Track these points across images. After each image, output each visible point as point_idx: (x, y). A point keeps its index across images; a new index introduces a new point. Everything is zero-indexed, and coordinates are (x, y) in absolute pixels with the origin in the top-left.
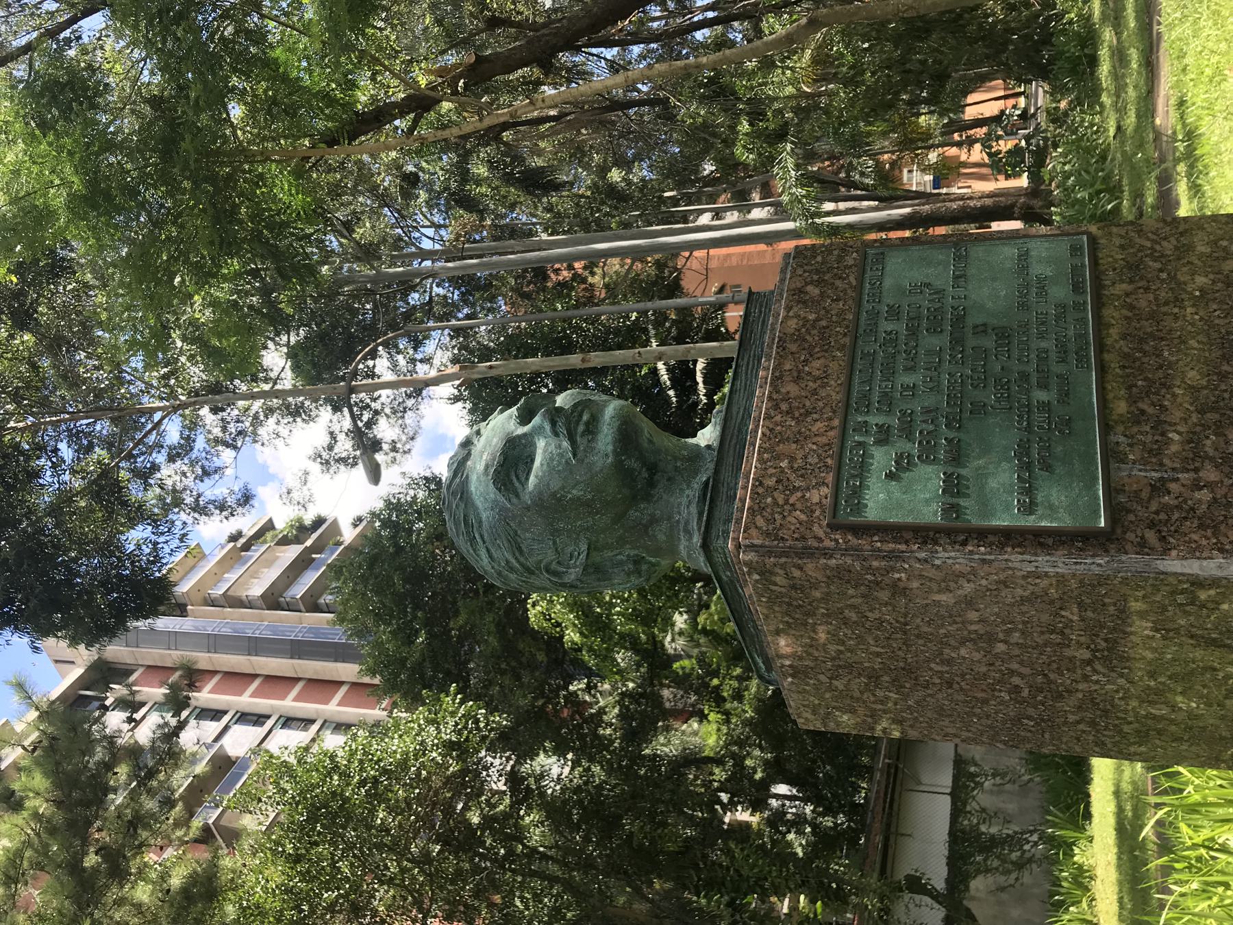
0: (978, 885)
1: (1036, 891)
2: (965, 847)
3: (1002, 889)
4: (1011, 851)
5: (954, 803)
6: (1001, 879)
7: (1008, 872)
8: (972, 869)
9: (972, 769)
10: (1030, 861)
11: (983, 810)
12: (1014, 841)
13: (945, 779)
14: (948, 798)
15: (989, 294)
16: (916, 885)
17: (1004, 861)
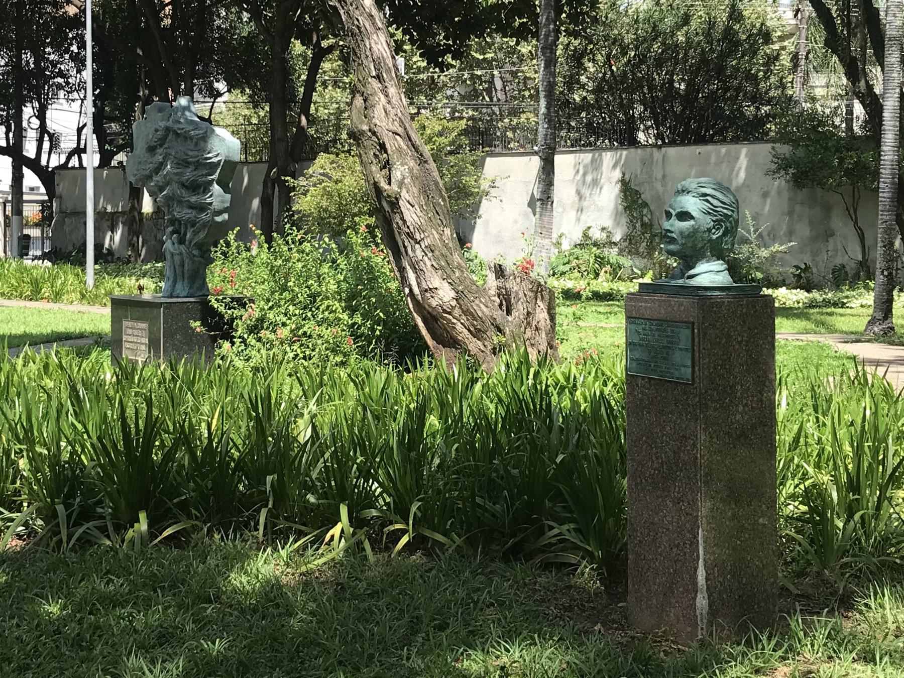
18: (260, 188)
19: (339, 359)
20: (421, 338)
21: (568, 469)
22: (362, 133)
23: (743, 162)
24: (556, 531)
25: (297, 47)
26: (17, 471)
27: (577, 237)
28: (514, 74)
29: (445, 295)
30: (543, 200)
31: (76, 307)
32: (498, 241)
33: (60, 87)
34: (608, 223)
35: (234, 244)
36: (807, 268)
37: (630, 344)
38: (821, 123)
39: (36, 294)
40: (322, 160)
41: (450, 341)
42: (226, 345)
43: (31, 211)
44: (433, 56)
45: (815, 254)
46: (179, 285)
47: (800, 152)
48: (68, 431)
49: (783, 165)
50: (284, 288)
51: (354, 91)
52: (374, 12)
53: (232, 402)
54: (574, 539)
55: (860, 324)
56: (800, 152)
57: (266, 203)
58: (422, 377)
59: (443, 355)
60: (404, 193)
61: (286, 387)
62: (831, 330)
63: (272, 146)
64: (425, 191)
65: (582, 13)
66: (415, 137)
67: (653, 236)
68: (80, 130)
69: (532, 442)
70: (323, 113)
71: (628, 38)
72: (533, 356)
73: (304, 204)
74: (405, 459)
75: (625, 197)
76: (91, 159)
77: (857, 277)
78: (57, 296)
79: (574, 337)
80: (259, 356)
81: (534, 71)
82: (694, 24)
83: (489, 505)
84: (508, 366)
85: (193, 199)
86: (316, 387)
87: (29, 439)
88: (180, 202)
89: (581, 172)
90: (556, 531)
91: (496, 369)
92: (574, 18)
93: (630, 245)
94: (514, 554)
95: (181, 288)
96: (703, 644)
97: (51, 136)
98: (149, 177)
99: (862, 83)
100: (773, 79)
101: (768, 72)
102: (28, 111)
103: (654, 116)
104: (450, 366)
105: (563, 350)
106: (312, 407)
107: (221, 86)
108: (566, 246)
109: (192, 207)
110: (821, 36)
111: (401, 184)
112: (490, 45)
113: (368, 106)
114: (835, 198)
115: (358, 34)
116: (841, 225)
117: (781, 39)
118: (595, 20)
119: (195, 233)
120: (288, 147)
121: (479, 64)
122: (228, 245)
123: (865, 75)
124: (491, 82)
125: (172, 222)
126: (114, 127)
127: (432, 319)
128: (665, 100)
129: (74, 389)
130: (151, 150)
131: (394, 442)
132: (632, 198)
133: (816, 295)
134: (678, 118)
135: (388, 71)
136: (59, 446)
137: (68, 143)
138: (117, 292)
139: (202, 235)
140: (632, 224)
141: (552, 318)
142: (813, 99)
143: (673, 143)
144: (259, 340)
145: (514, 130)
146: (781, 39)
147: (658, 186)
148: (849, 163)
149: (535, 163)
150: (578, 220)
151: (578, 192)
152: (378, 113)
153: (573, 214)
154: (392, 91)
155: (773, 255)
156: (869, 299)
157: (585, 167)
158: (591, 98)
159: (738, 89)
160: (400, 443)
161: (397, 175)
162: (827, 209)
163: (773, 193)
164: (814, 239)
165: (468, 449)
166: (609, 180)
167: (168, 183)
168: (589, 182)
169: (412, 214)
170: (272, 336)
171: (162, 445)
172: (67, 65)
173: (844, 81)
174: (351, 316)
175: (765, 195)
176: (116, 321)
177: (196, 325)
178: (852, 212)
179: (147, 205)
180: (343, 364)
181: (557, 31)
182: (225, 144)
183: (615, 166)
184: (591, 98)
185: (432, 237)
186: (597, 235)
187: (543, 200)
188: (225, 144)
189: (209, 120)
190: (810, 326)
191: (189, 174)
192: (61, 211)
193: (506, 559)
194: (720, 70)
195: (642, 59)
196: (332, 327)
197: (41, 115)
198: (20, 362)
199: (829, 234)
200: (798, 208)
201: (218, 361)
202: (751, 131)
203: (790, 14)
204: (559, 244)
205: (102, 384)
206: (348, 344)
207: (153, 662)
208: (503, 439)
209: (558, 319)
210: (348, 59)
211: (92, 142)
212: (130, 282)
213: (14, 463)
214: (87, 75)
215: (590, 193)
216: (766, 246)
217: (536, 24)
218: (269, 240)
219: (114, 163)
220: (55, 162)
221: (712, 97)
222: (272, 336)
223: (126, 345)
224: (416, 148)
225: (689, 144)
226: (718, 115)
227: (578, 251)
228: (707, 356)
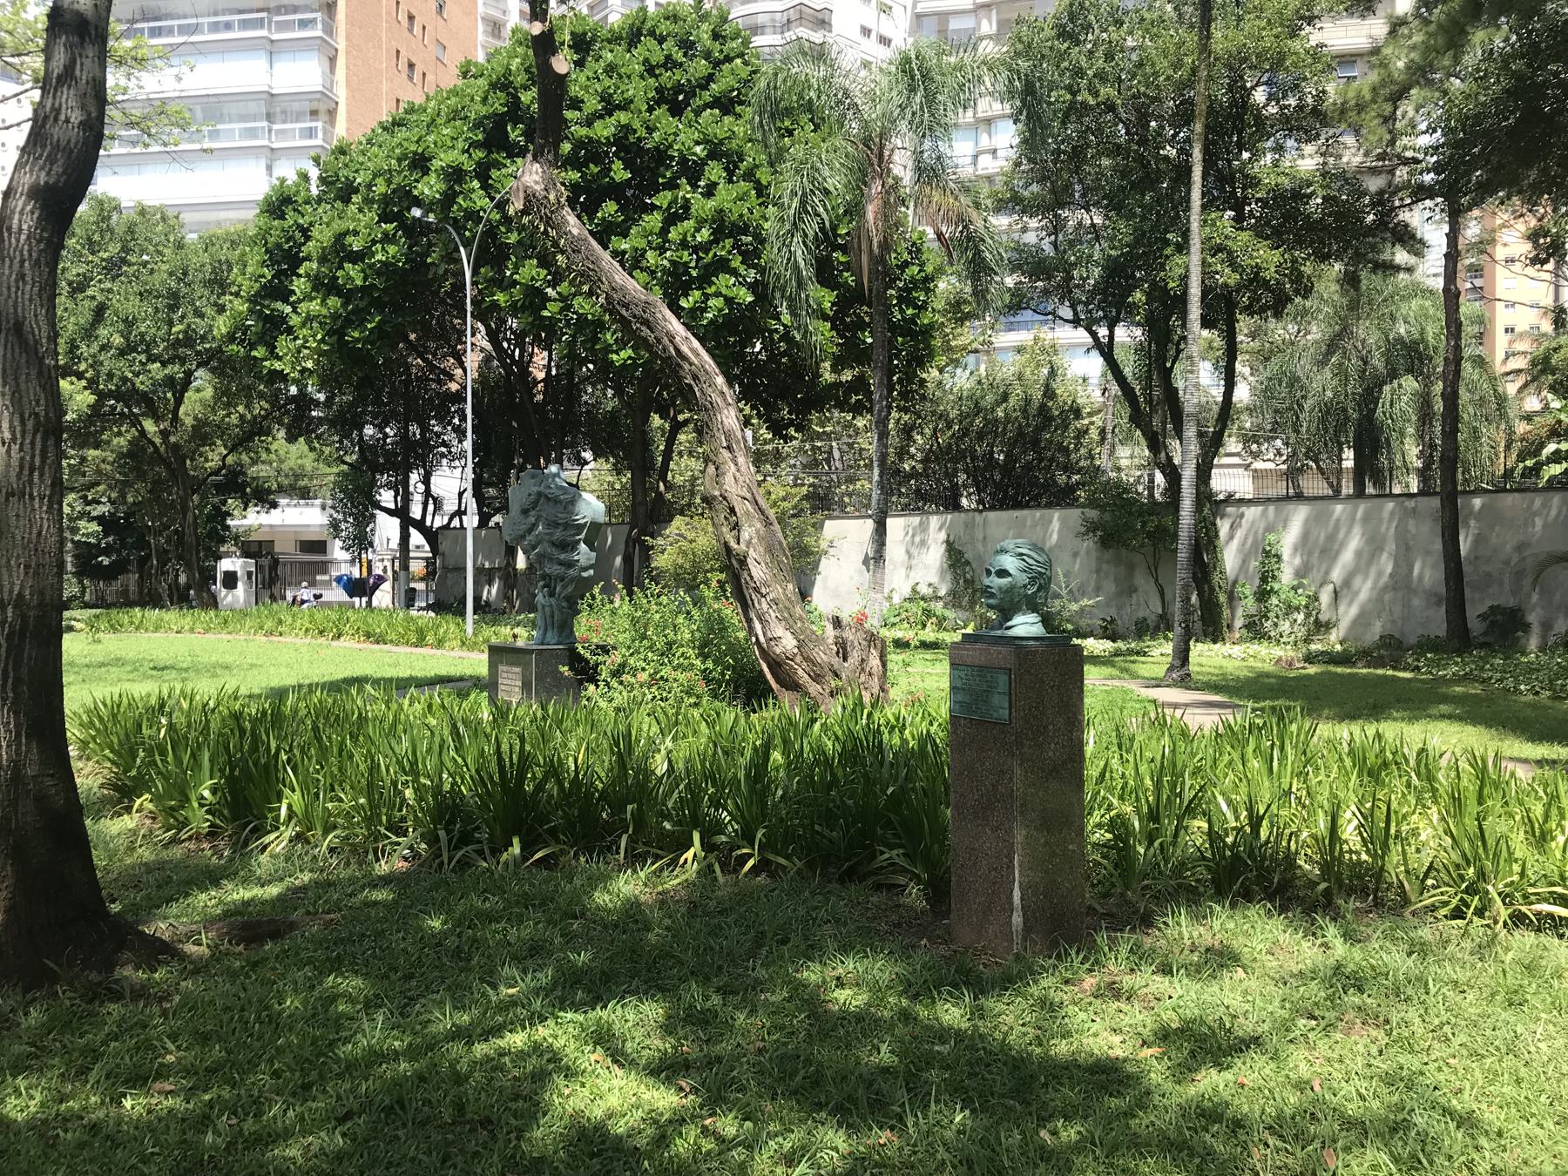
18: (622, 547)
19: (692, 700)
20: (767, 682)
21: (897, 800)
22: (714, 498)
23: (1056, 525)
24: (886, 856)
25: (656, 420)
26: (404, 800)
27: (907, 592)
28: (851, 446)
29: (788, 643)
30: (876, 558)
31: (457, 653)
32: (836, 594)
33: (443, 455)
34: (935, 580)
35: (598, 597)
36: (1113, 621)
37: (953, 688)
38: (1126, 491)
39: (420, 642)
40: (678, 521)
41: (792, 685)
42: (592, 687)
43: (417, 567)
44: (778, 429)
45: (1120, 608)
46: (549, 634)
47: (1107, 517)
48: (449, 764)
49: (1091, 528)
50: (644, 637)
51: (707, 460)
52: (725, 389)
53: (597, 739)
54: (902, 862)
55: (1160, 671)
56: (1107, 517)
57: (628, 560)
58: (767, 716)
59: (786, 697)
60: (751, 552)
61: (645, 726)
62: (1134, 676)
63: (633, 510)
64: (770, 550)
65: (912, 391)
66: (761, 502)
67: (975, 591)
68: (461, 495)
69: (866, 775)
70: (679, 480)
71: (953, 414)
72: (867, 699)
73: (661, 561)
74: (752, 790)
75: (950, 557)
76: (472, 521)
77: (1157, 629)
78: (440, 643)
79: (903, 681)
80: (621, 697)
81: (869, 443)
82: (1012, 401)
83: (826, 832)
84: (844, 707)
85: (562, 557)
86: (671, 726)
87: (414, 772)
88: (551, 559)
90: (886, 856)
91: (834, 709)
92: (904, 395)
93: (954, 599)
94: (848, 877)
95: (551, 636)
96: (1018, 957)
97: (435, 500)
98: (523, 537)
99: (1163, 455)
100: (1083, 451)
101: (1078, 445)
102: (414, 477)
103: (976, 484)
104: (792, 707)
105: (893, 693)
106: (669, 743)
107: (588, 455)
108: (896, 600)
109: (561, 563)
110: (1126, 412)
111: (749, 543)
112: (829, 420)
113: (719, 473)
114: (1137, 558)
115: (710, 409)
116: (1143, 582)
117: (1090, 414)
118: (923, 398)
119: (564, 587)
120: (647, 510)
121: (819, 436)
122: (593, 598)
123: (1166, 447)
124: (830, 453)
125: (543, 577)
126: (492, 491)
127: (776, 665)
128: (986, 469)
129: (454, 727)
130: (525, 512)
131: (741, 775)
132: (956, 557)
133: (1120, 644)
134: (997, 486)
135: (738, 442)
136: (441, 778)
137: (450, 506)
138: (494, 640)
139: (570, 589)
140: (956, 580)
141: (884, 664)
142: (1119, 469)
143: (993, 508)
144: (621, 683)
145: (850, 495)
146: (1090, 414)
147: (980, 546)
148: (1150, 527)
149: (869, 525)
151: (908, 552)
152: (728, 480)
153: (903, 571)
154: (741, 460)
155: (1082, 609)
156: (1168, 648)
158: (919, 467)
159: (1052, 460)
160: (747, 776)
161: (745, 535)
162: (1131, 567)
163: (1082, 553)
164: (1119, 594)
165: (808, 781)
166: (935, 540)
167: (539, 543)
168: (918, 542)
169: (758, 571)
170: (633, 680)
171: (534, 778)
172: (450, 436)
173: (1147, 452)
174: (703, 662)
175: (1075, 555)
176: (493, 666)
177: (565, 669)
178: (1153, 571)
179: (521, 562)
180: (696, 705)
181: (890, 407)
182: (591, 507)
183: (940, 529)
184: (919, 467)
185: (776, 591)
186: (924, 590)
187: (876, 558)
188: (591, 507)
189: (576, 486)
190: (1115, 672)
191: (558, 534)
192: (444, 567)
193: (841, 881)
194: (1035, 442)
195: (965, 432)
196: (687, 671)
197: (426, 481)
198: (406, 702)
199: (1133, 590)
200: (1105, 567)
201: (584, 702)
202: (1062, 497)
203: (1098, 393)
204: (890, 598)
205: (480, 722)
206: (701, 688)
207: (525, 972)
208: (840, 773)
209: (889, 665)
210: (701, 431)
211: (472, 506)
212: (506, 631)
213: (401, 792)
214: (468, 445)
215: (918, 552)
216: (1076, 601)
217: (871, 400)
218: (630, 594)
219: (491, 524)
220: (438, 522)
221: (1028, 467)
222: (633, 680)
223: (501, 687)
224: (763, 512)
225: (1007, 509)
226: (1034, 483)
227: (907, 605)
228: (1022, 699)
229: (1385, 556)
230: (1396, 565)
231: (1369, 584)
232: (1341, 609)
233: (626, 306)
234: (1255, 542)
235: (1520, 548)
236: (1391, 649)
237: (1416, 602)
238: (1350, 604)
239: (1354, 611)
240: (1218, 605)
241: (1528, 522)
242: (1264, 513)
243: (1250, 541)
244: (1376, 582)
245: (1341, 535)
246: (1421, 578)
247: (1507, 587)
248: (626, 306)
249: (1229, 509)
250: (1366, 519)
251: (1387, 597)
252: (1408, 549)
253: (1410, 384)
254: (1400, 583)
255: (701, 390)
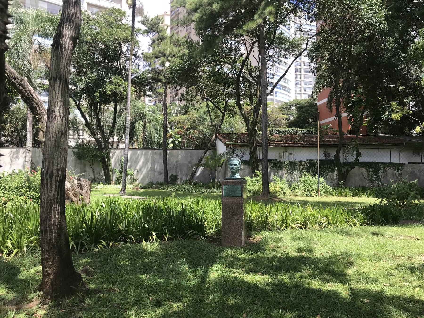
0: (363, 170)
1: (364, 183)
2: (374, 167)
3: (363, 175)
4: (375, 178)
5: (388, 163)
6: (366, 175)
7: (368, 177)
8: (368, 168)
9: (400, 168)
10: (373, 182)
11: (387, 171)
12: (378, 178)
13: (395, 160)
14: (390, 162)
15: (237, 192)
16: (359, 155)
17: (371, 176)
27: (10, 172)
89: (12, 154)
150: (11, 167)
151: (11, 160)
157: (14, 153)
166: (22, 156)
183: (23, 153)
229: (149, 163)
230: (152, 165)
231: (145, 170)
232: (139, 176)
233: (15, 79)
234: (118, 159)
235: (177, 162)
236: (150, 185)
237: (156, 174)
238: (141, 175)
239: (142, 176)
240: (110, 175)
241: (178, 156)
242: (121, 152)
243: (117, 159)
244: (147, 169)
245: (139, 158)
246: (157, 168)
247: (174, 170)
248: (15, 79)
249: (112, 151)
250: (145, 154)
251: (149, 173)
252: (154, 162)
253: (142, 123)
254: (152, 170)
255: (39, 108)
